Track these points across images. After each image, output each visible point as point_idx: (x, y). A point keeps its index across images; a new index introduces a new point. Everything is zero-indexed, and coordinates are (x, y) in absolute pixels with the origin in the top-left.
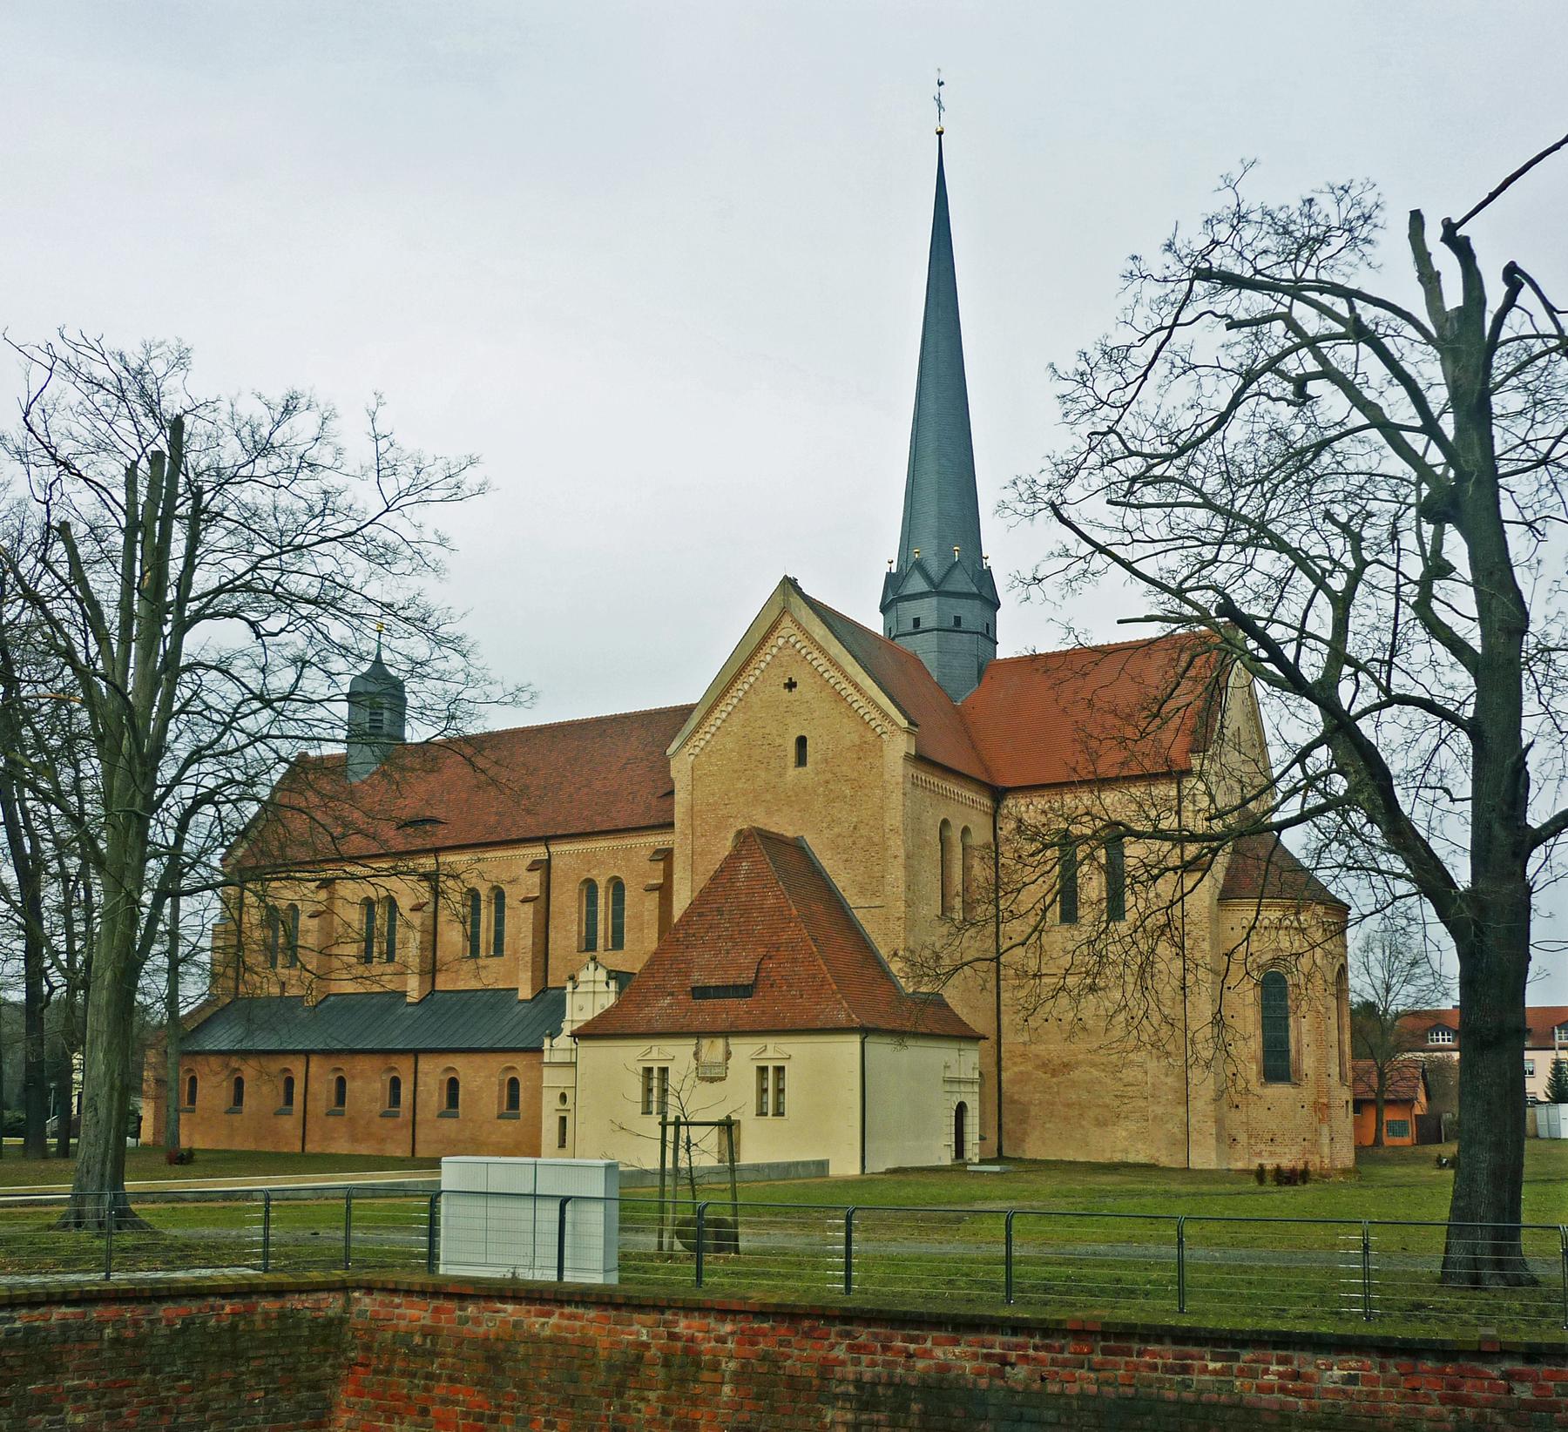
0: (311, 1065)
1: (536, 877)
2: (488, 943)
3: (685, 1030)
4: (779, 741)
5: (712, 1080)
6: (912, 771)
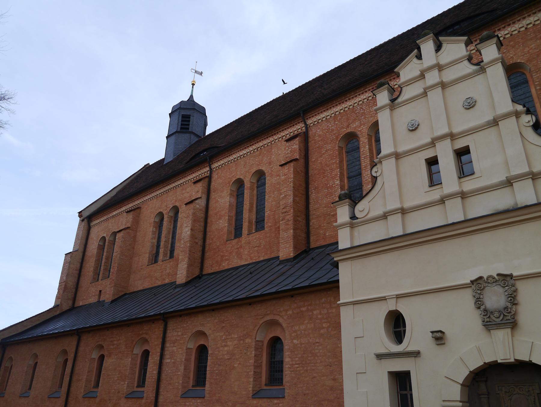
1: (296, 145)
2: (250, 222)
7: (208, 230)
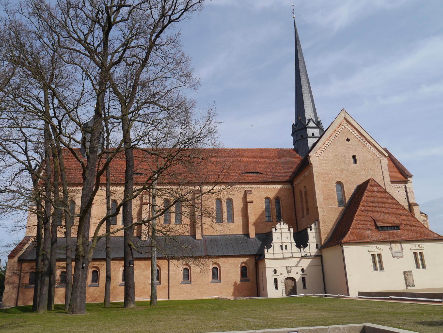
0: (170, 263)
3: (386, 240)
4: (347, 156)
5: (398, 257)
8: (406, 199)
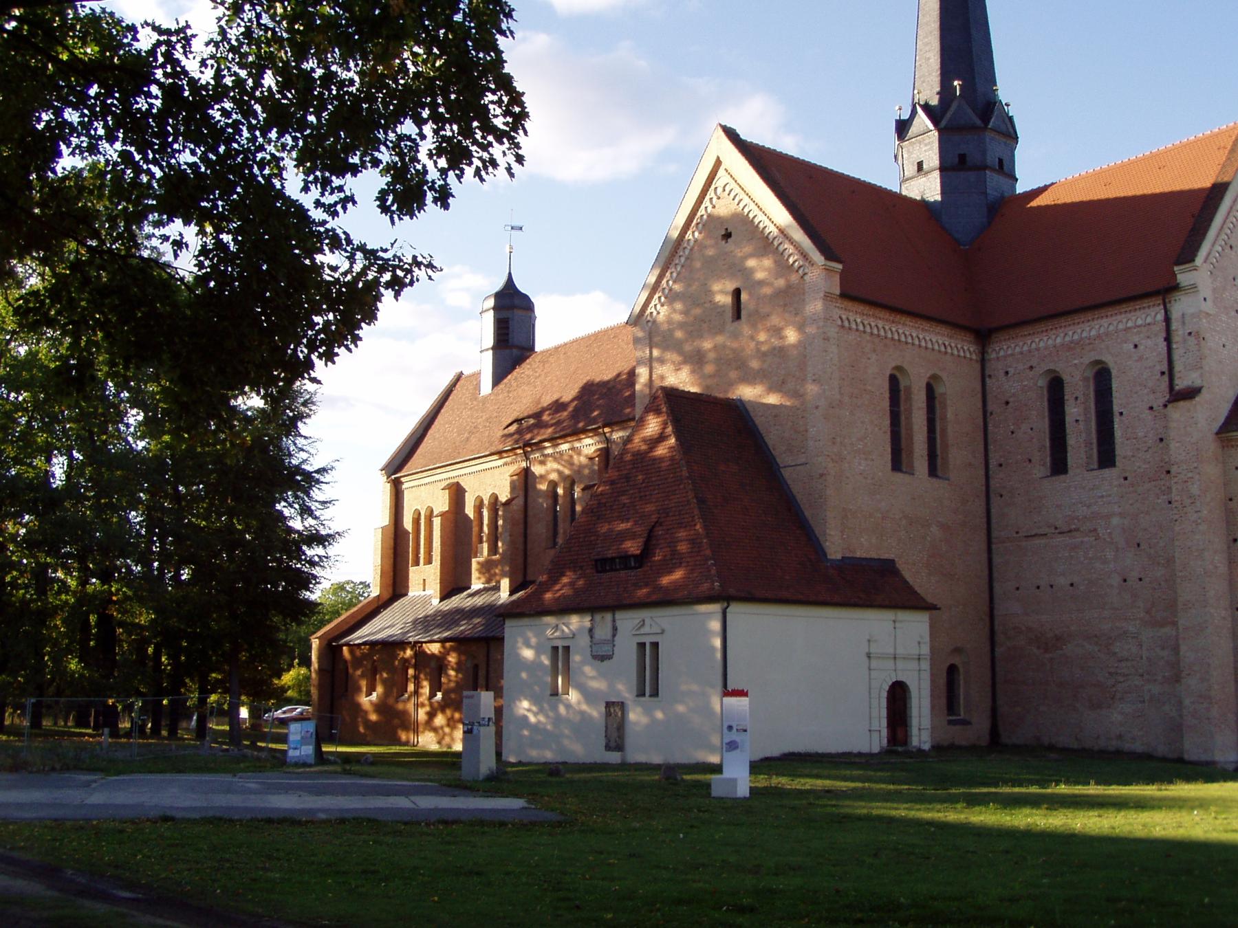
6: (836, 313)
7: (529, 532)
8: (1163, 373)
